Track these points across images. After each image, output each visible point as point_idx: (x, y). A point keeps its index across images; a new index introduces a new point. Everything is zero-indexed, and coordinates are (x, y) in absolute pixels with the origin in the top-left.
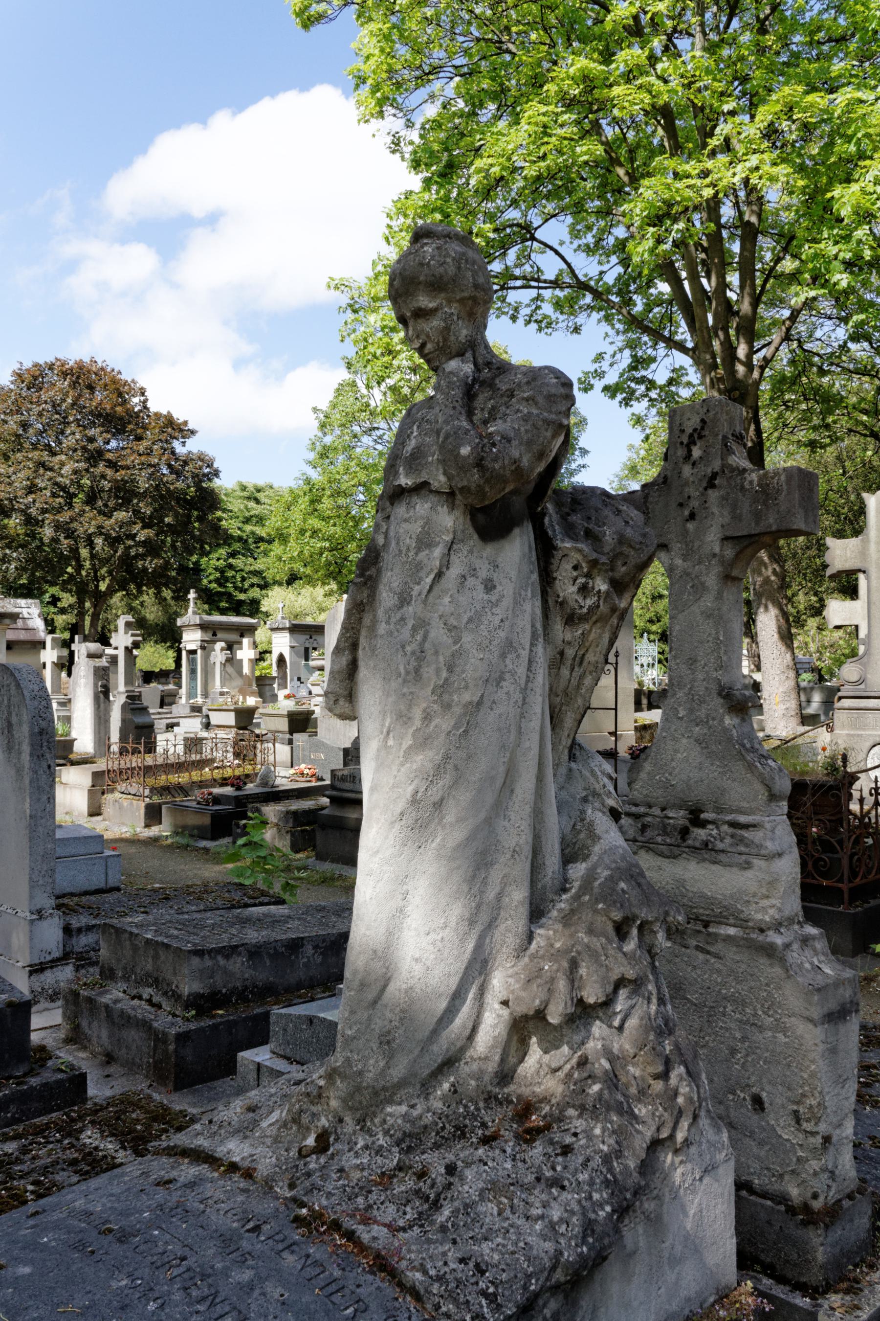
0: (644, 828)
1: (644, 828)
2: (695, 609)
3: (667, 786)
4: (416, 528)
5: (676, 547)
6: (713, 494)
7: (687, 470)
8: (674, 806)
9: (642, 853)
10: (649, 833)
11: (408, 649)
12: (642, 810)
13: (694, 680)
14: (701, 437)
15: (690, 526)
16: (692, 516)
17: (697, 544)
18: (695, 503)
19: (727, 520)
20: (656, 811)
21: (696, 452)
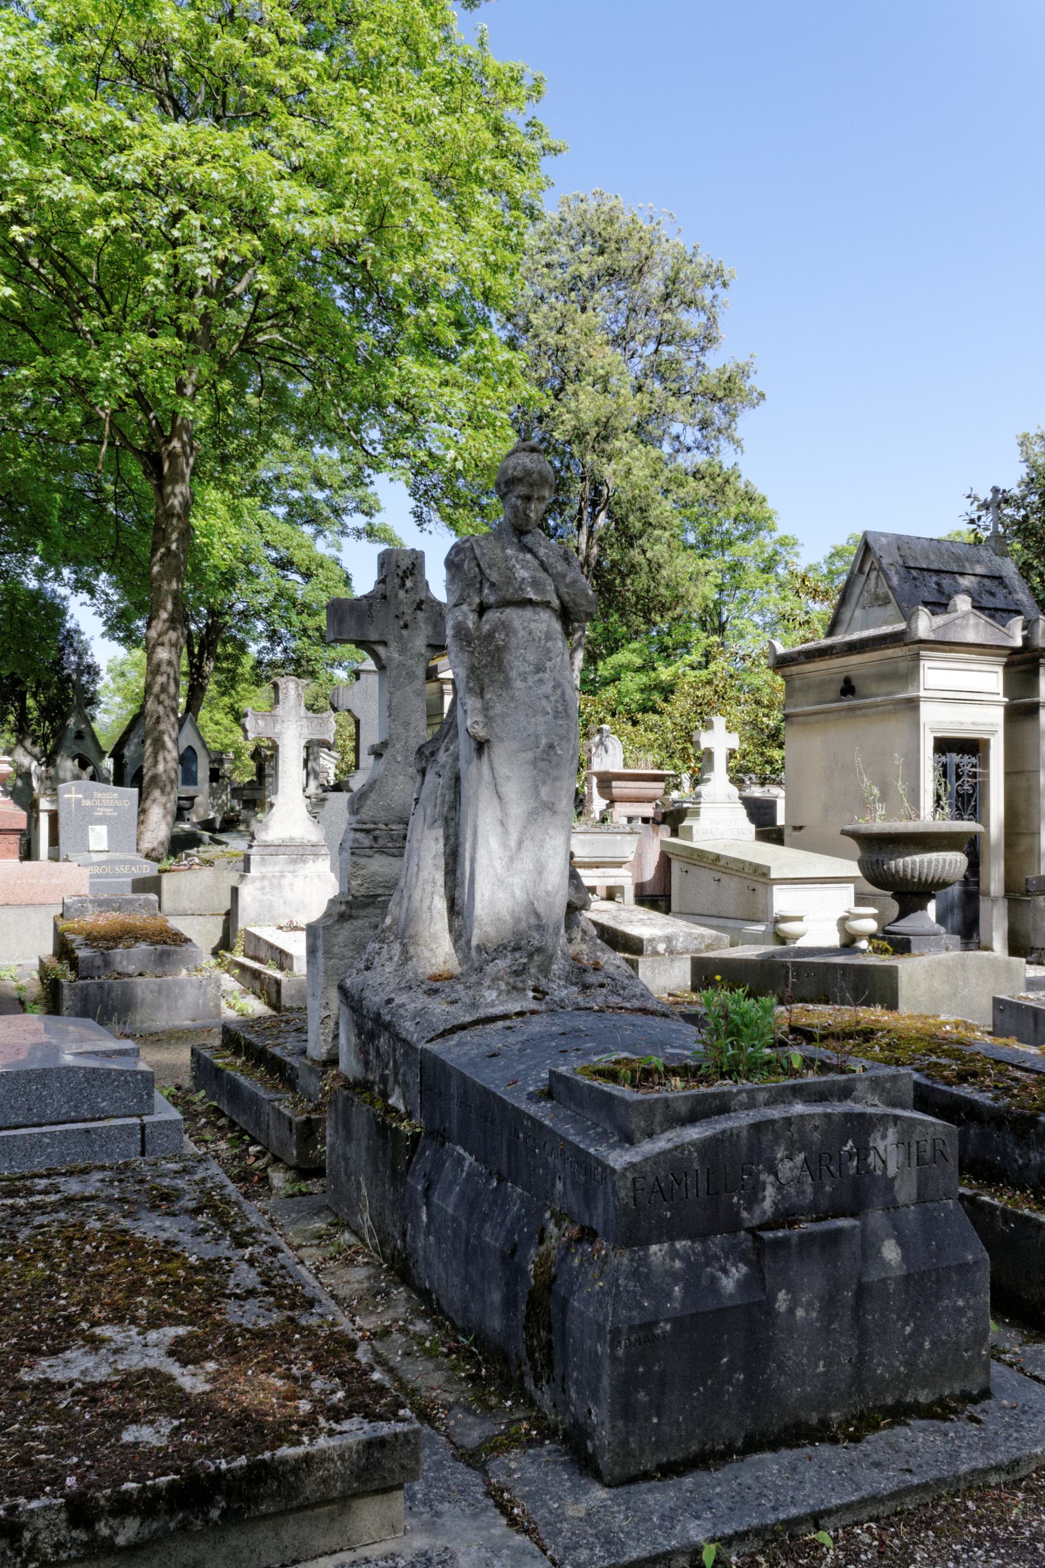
0: (376, 839)
1: (376, 839)
2: (408, 688)
3: (388, 809)
4: (543, 627)
5: (393, 645)
6: (420, 615)
7: (402, 594)
8: (393, 822)
9: (377, 856)
10: (381, 842)
11: (552, 699)
12: (372, 826)
13: (407, 737)
14: (412, 574)
15: (404, 632)
16: (406, 626)
17: (410, 645)
18: (408, 618)
19: (431, 633)
20: (383, 827)
21: (409, 584)
